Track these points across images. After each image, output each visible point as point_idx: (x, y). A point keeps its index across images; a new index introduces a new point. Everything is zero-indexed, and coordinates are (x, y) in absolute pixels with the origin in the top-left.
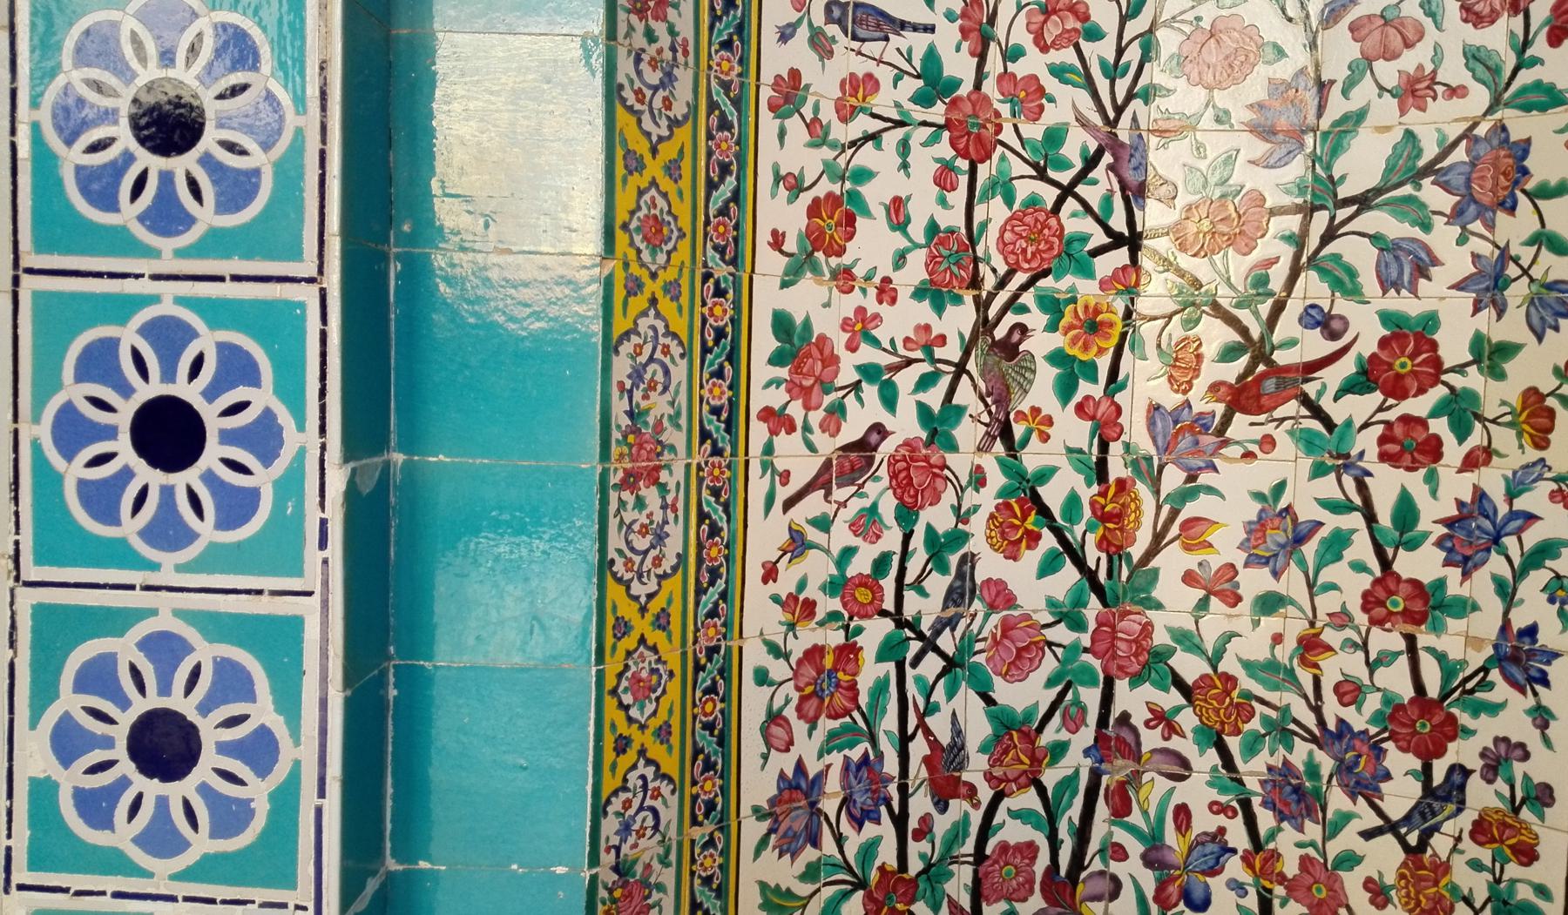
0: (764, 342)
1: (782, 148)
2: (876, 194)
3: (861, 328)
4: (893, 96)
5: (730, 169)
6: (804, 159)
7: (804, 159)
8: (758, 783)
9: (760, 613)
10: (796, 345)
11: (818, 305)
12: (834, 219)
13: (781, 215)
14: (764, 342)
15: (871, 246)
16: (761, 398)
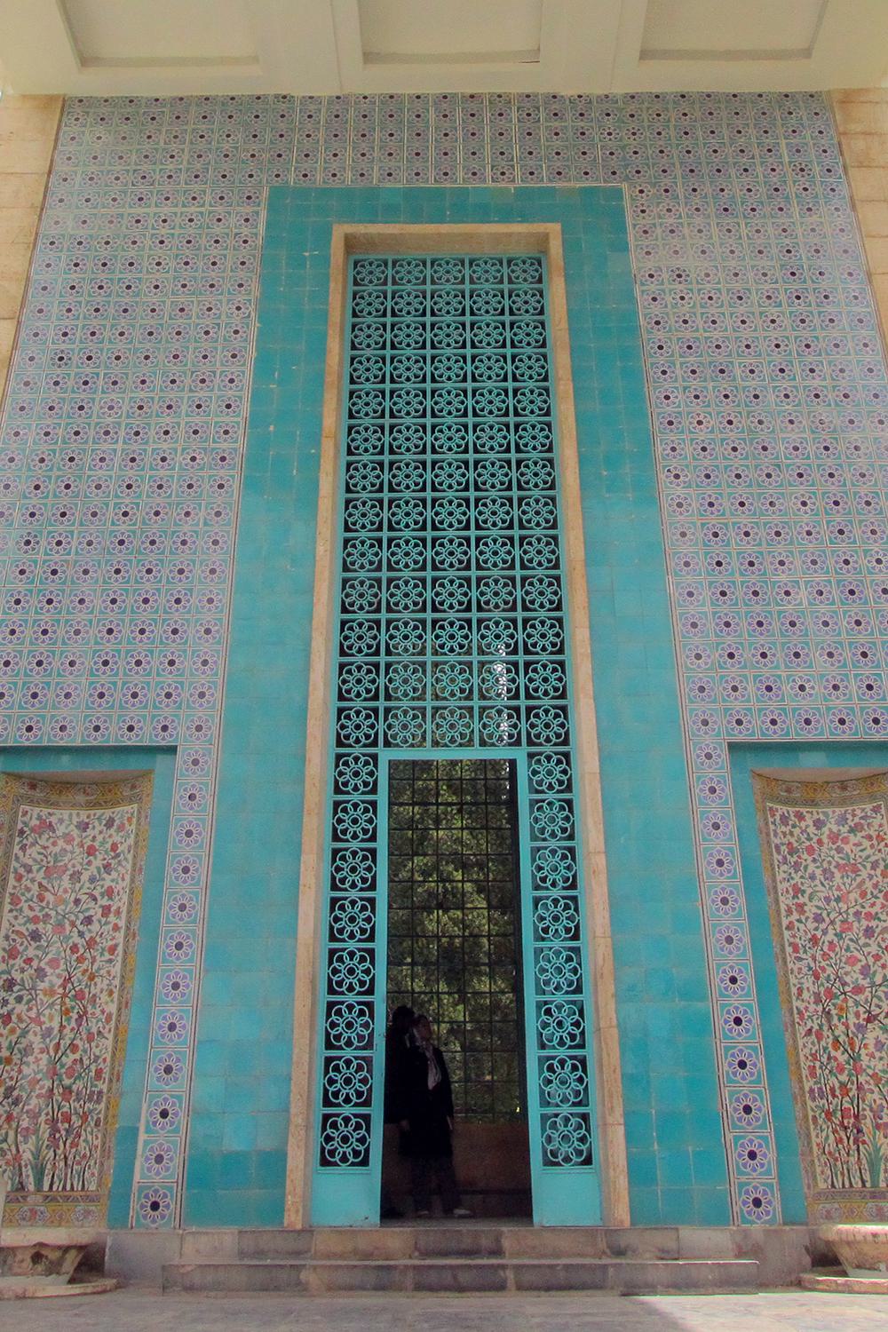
0: (795, 1011)
1: (793, 980)
2: (805, 986)
3: (806, 1009)
4: (805, 970)
5: (788, 983)
6: (796, 981)
7: (796, 981)
8: (807, 1089)
9: (802, 1058)
10: (800, 1013)
11: (802, 1006)
12: (800, 991)
13: (794, 990)
14: (795, 1011)
15: (805, 995)
16: (797, 1020)
